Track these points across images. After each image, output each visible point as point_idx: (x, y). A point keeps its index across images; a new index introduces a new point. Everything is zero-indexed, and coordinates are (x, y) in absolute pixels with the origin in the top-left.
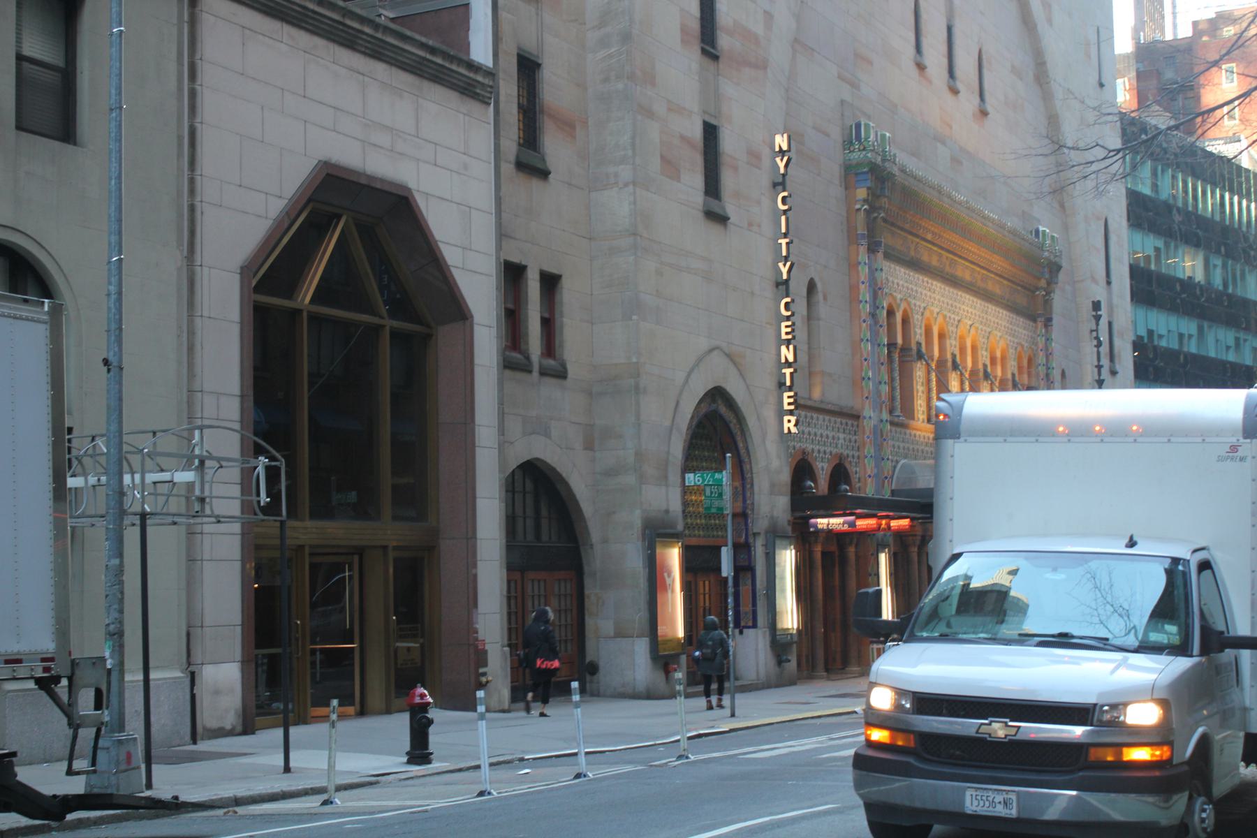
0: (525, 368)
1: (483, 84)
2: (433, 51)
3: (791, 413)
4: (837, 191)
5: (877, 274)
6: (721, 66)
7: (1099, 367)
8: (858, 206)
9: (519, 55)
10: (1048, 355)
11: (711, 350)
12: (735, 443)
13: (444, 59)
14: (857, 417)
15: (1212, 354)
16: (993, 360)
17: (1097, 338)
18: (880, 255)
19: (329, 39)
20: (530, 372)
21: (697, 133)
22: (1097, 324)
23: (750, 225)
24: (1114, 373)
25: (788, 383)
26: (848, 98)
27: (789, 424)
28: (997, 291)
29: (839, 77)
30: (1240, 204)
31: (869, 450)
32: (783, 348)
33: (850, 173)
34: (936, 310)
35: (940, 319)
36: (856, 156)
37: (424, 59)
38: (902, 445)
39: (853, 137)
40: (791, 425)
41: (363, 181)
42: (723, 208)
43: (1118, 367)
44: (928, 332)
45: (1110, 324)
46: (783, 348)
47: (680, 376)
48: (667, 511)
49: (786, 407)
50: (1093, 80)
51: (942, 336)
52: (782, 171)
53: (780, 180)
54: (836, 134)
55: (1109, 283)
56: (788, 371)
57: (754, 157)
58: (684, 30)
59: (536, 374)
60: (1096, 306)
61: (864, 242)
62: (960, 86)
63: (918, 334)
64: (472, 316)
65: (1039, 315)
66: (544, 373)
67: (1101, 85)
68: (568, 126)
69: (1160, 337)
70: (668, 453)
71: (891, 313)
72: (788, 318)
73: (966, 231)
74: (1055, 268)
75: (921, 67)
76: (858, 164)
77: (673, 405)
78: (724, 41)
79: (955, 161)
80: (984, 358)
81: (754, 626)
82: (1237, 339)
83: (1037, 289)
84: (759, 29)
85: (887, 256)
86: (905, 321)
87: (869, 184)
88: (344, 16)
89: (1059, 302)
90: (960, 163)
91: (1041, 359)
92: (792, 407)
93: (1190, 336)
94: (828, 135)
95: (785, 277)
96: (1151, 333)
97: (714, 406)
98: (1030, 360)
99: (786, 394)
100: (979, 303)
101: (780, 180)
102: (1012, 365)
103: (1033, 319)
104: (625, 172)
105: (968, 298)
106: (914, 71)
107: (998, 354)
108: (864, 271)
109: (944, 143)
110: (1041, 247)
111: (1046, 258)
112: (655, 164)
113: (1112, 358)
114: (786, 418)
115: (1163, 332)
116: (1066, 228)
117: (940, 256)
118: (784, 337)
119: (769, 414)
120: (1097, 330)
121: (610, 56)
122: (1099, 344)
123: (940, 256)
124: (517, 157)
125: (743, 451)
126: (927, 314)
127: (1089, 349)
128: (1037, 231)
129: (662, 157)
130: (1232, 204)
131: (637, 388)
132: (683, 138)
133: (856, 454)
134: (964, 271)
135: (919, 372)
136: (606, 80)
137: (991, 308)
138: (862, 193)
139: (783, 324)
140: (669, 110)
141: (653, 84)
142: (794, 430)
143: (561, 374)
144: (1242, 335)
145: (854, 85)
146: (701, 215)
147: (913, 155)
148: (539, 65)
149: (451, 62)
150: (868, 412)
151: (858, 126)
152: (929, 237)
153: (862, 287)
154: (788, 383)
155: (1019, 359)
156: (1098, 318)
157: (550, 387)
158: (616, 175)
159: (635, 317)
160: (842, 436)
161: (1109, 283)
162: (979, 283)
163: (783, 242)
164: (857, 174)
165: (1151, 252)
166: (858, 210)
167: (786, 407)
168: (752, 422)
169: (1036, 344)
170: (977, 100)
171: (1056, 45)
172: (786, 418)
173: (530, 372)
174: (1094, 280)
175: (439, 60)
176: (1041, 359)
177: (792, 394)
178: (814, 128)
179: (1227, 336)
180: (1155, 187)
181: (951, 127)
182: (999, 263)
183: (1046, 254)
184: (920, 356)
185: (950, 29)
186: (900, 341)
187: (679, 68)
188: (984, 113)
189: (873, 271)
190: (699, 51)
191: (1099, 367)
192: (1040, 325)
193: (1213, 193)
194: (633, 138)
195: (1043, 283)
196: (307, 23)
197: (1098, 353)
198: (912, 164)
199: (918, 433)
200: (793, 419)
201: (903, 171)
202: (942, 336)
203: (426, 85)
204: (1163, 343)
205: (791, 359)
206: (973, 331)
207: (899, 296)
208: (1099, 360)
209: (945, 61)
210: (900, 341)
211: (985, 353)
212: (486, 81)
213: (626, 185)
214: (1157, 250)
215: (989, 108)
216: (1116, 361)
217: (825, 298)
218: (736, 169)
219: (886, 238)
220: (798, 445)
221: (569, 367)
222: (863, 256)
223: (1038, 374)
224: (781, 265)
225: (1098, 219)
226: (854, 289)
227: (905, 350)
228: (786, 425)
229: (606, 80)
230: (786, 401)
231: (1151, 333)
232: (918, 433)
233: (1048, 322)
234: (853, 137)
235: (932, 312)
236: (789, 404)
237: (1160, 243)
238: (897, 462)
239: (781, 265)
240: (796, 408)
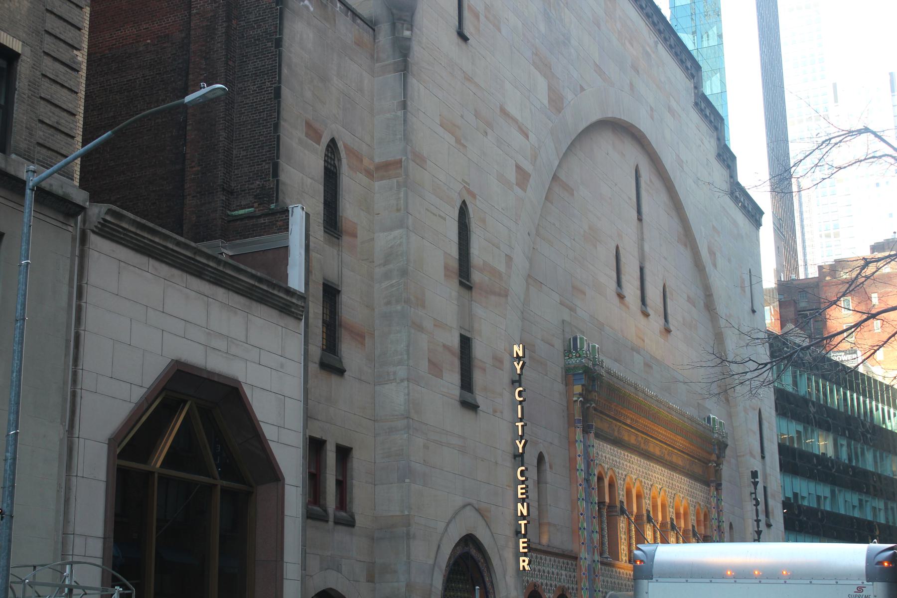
0: (324, 518)
2: (260, 280)
3: (525, 554)
4: (560, 387)
5: (590, 449)
6: (473, 293)
7: (758, 521)
8: (575, 399)
9: (324, 284)
10: (719, 511)
11: (464, 506)
12: (482, 577)
13: (268, 286)
14: (575, 558)
15: (842, 512)
16: (678, 515)
17: (756, 499)
18: (592, 435)
19: (183, 270)
20: (327, 521)
21: (455, 342)
22: (755, 489)
23: (495, 411)
24: (769, 525)
25: (523, 532)
26: (567, 318)
27: (524, 563)
29: (562, 303)
30: (858, 399)
31: (585, 583)
32: (519, 505)
33: (569, 374)
34: (634, 477)
35: (637, 484)
36: (574, 361)
37: (253, 285)
38: (609, 580)
39: (572, 347)
40: (525, 564)
41: (205, 376)
42: (475, 400)
43: (772, 521)
44: (629, 493)
45: (765, 488)
46: (519, 505)
47: (441, 526)
49: (522, 550)
50: (748, 307)
51: (639, 497)
52: (519, 372)
53: (517, 378)
54: (559, 345)
55: (763, 457)
56: (523, 523)
57: (498, 361)
58: (446, 268)
59: (331, 523)
60: (754, 474)
61: (580, 425)
63: (621, 495)
64: (284, 479)
65: (712, 482)
66: (337, 522)
67: (754, 311)
68: (359, 336)
69: (803, 498)
70: (431, 585)
71: (600, 479)
72: (523, 482)
73: (655, 418)
74: (722, 446)
75: (621, 297)
76: (575, 368)
77: (435, 549)
78: (476, 276)
79: (647, 365)
80: (671, 513)
82: (860, 501)
83: (710, 461)
84: (502, 268)
85: (597, 436)
86: (612, 485)
87: (583, 382)
88: (195, 254)
89: (726, 470)
90: (650, 367)
91: (714, 514)
92: (526, 550)
93: (825, 498)
94: (553, 346)
95: (521, 451)
96: (795, 495)
97: (466, 549)
98: (705, 515)
99: (521, 540)
100: (666, 472)
101: (517, 378)
102: (692, 519)
103: (707, 483)
104: (402, 372)
105: (658, 468)
106: (616, 300)
107: (682, 511)
108: (580, 447)
109: (638, 353)
110: (712, 430)
111: (717, 439)
112: (424, 365)
113: (767, 515)
114: (521, 559)
115: (805, 494)
116: (730, 416)
117: (637, 436)
118: (520, 496)
119: (509, 555)
120: (755, 493)
121: (392, 286)
122: (757, 504)
123: (637, 436)
124: (321, 359)
125: (488, 584)
126: (628, 479)
127: (750, 506)
128: (709, 418)
129: (429, 361)
130: (852, 399)
131: (408, 534)
132: (444, 346)
133: (575, 587)
134: (655, 448)
135: (622, 524)
136: (388, 303)
137: (676, 476)
138: (578, 389)
139: (520, 487)
140: (435, 325)
141: (424, 307)
142: (527, 568)
143: (350, 523)
144: (864, 497)
145: (572, 309)
146: (457, 404)
147: (616, 360)
148: (339, 292)
149: (274, 289)
150: (584, 554)
151: (575, 339)
152: (628, 422)
153: (579, 459)
154: (523, 532)
155: (698, 514)
156: (755, 484)
157: (341, 534)
158: (395, 373)
159: (407, 480)
160: (564, 573)
161: (763, 457)
162: (667, 457)
163: (520, 424)
164: (574, 375)
165: (794, 435)
166: (576, 401)
167: (522, 550)
168: (495, 561)
171: (720, 282)
172: (521, 559)
175: (265, 288)
176: (714, 514)
177: (526, 540)
178: (542, 340)
179: (854, 498)
180: (795, 383)
181: (644, 341)
182: (680, 442)
183: (716, 435)
184: (623, 512)
185: (642, 270)
186: (607, 500)
187: (442, 297)
188: (668, 331)
189: (587, 447)
190: (458, 283)
191: (758, 521)
193: (838, 391)
194: (408, 346)
195: (714, 457)
196: (167, 258)
197: (757, 511)
198: (615, 368)
199: (622, 571)
200: (527, 559)
201: (608, 372)
202: (639, 497)
203: (255, 305)
204: (806, 503)
205: (525, 513)
206: (662, 493)
207: (606, 466)
208: (757, 516)
209: (639, 292)
210: (607, 500)
211: (671, 510)
212: (299, 303)
213: (402, 381)
214: (798, 432)
215: (672, 328)
216: (771, 517)
217: (551, 467)
218: (484, 370)
219: (596, 423)
220: (530, 580)
221: (357, 517)
222: (579, 435)
223: (712, 526)
224: (517, 442)
225: (754, 409)
226: (572, 461)
227: (611, 507)
228: (522, 564)
229: (388, 303)
230: (522, 545)
231: (795, 495)
232: (622, 571)
233: (718, 487)
234: (572, 347)
235: (631, 478)
236: (524, 548)
237: (800, 428)
238: (606, 593)
239: (517, 442)
240: (529, 551)
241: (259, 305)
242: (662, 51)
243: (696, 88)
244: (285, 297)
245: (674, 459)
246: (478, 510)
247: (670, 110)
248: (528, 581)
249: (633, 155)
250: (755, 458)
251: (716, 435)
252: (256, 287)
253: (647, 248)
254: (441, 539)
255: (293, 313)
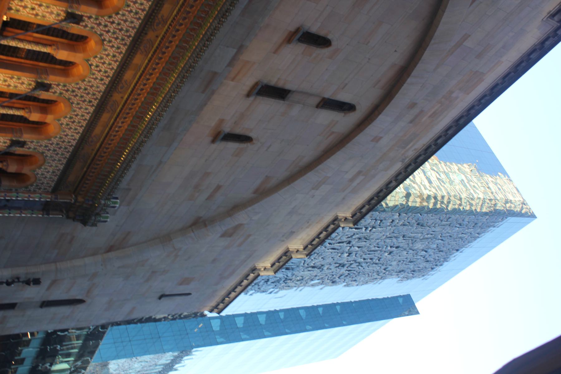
16: (46, 106)
17: (13, 282)
22: (23, 282)
28: (98, 130)
45: (12, 306)
60: (37, 282)
62: (252, 98)
67: (160, 297)
75: (289, 39)
83: (76, 196)
91: (23, 196)
103: (55, 191)
106: (292, 28)
107: (49, 118)
109: (231, 64)
120: (19, 281)
128: (117, 198)
169: (35, 192)
170: (227, 129)
174: (54, 282)
181: (233, 80)
183: (103, 202)
192: (47, 198)
223: (10, 191)
233: (47, 208)
242: (398, 166)
243: (346, 219)
245: (105, 117)
247: (359, 173)
249: (363, 106)
250: (49, 288)
251: (103, 202)
253: (296, 111)
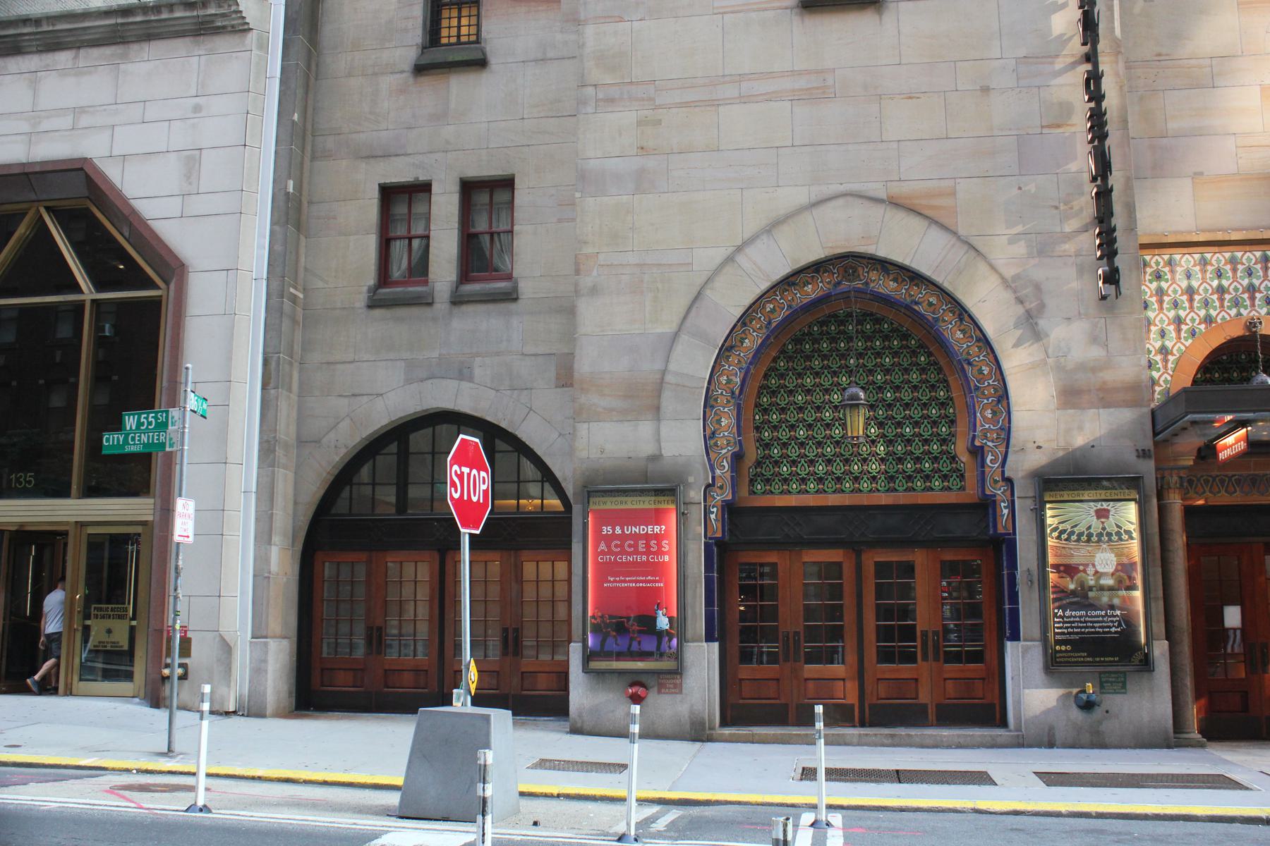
0: (425, 301)
1: (223, 15)
37: (117, 24)
47: (709, 257)
48: (655, 458)
59: (442, 304)
66: (458, 300)
70: (664, 372)
81: (1015, 637)
143: (511, 296)
173: (430, 304)
203: (135, 47)
241: (145, 46)
244: (188, 14)
246: (895, 203)
248: (1208, 320)
252: (122, 24)
254: (709, 280)
255: (224, 27)
